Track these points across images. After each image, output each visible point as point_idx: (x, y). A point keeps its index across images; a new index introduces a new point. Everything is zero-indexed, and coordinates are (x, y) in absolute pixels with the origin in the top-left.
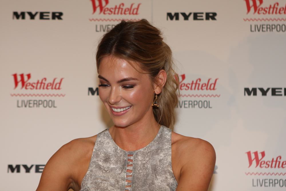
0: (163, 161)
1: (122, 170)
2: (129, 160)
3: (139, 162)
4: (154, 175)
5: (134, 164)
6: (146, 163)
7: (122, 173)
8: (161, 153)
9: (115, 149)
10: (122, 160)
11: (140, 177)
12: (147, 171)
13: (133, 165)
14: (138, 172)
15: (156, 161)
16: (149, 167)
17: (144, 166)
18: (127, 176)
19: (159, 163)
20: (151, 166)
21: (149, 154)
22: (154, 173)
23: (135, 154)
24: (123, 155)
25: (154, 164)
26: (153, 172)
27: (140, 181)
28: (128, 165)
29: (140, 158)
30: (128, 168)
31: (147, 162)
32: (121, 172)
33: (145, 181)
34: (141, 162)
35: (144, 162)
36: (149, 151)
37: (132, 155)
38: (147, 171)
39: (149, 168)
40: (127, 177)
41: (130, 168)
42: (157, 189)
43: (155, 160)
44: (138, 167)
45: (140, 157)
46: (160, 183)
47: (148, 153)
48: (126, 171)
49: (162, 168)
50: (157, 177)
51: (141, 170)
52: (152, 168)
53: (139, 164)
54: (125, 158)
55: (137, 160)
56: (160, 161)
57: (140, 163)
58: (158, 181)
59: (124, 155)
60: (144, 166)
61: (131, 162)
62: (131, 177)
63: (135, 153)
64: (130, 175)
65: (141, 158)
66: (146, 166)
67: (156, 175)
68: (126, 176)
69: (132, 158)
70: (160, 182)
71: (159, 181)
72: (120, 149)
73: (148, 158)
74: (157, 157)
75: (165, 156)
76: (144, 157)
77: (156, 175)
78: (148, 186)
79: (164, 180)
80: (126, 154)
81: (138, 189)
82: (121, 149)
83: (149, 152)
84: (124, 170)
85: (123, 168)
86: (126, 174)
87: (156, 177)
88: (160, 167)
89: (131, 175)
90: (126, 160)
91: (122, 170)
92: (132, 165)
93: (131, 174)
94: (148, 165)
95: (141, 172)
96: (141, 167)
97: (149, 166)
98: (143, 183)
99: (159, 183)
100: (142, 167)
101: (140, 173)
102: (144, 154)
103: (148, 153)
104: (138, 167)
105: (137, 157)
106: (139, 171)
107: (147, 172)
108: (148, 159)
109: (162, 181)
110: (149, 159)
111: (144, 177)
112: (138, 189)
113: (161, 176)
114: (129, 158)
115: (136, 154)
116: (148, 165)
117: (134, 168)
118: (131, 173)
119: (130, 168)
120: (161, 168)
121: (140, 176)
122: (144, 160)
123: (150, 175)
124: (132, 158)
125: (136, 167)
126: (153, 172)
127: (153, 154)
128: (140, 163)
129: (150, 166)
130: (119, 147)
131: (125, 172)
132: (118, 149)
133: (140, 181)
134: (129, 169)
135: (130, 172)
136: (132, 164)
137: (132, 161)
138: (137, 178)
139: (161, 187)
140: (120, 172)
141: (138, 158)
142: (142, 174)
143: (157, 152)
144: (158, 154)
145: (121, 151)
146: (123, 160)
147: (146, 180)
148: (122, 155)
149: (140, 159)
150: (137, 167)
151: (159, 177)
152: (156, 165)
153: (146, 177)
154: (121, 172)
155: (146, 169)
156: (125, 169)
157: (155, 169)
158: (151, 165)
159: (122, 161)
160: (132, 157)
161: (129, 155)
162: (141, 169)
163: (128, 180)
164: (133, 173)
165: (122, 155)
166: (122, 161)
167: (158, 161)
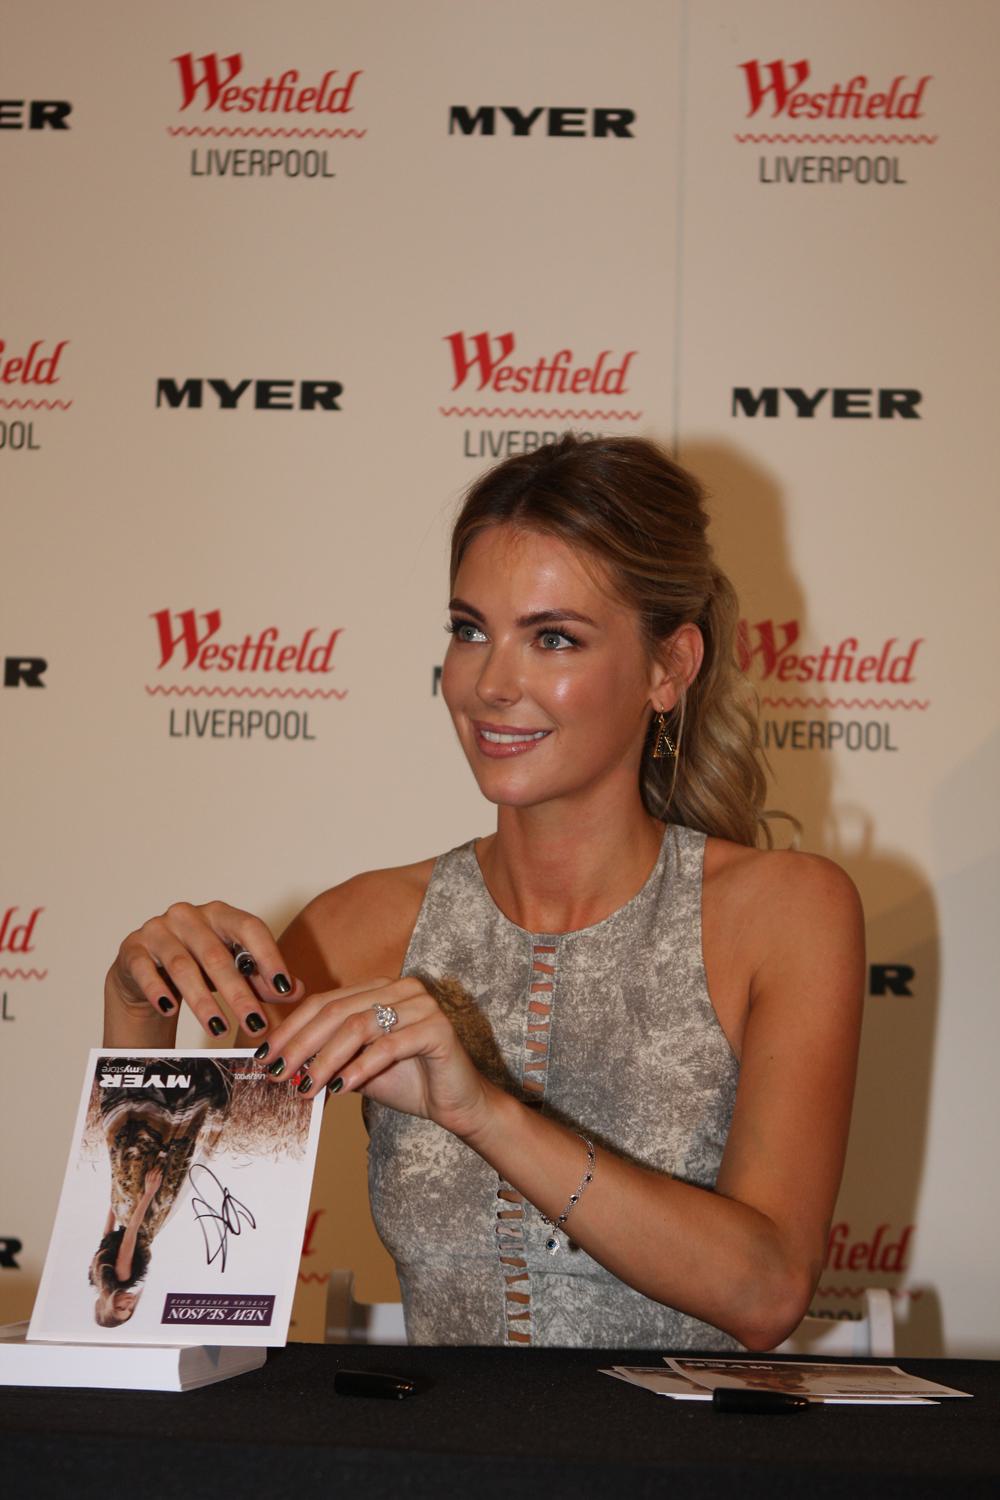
0: (673, 970)
1: (512, 1005)
2: (538, 965)
4: (637, 1029)
5: (558, 983)
6: (607, 977)
7: (511, 1016)
8: (662, 939)
9: (491, 922)
10: (510, 962)
12: (607, 1009)
13: (555, 986)
14: (570, 1011)
15: (644, 972)
16: (613, 995)
17: (595, 990)
18: (529, 1026)
19: (654, 980)
20: (624, 995)
21: (618, 947)
22: (637, 1020)
24: (515, 946)
25: (638, 985)
26: (632, 1018)
27: (578, 1047)
28: (535, 988)
29: (581, 960)
30: (533, 997)
31: (612, 974)
32: (509, 1011)
33: (597, 1049)
34: (586, 976)
35: (597, 975)
36: (619, 935)
37: (552, 950)
38: (607, 1009)
39: (615, 998)
41: (544, 997)
44: (574, 993)
46: (659, 1059)
49: (671, 998)
50: (650, 1033)
51: (584, 1004)
52: (627, 1002)
53: (578, 982)
54: (525, 959)
55: (569, 968)
56: (660, 970)
57: (580, 977)
58: (651, 1049)
59: (519, 947)
61: (545, 976)
63: (564, 942)
64: (543, 1023)
65: (586, 962)
66: (604, 990)
68: (525, 1028)
70: (656, 1055)
71: (656, 1048)
72: (504, 924)
74: (648, 955)
75: (677, 952)
76: (600, 960)
77: (643, 1027)
78: (609, 1069)
80: (526, 943)
82: (508, 923)
83: (617, 940)
84: (520, 1004)
86: (526, 1018)
87: (645, 1036)
88: (663, 992)
90: (525, 967)
91: (512, 1005)
92: (548, 986)
93: (547, 1020)
94: (614, 988)
96: (583, 994)
97: (616, 991)
98: (590, 1053)
99: (654, 1058)
102: (599, 948)
104: (572, 995)
106: (574, 1008)
107: (605, 1014)
108: (614, 963)
109: (664, 1051)
110: (619, 964)
111: (593, 1031)
113: (667, 1030)
114: (541, 957)
115: (567, 947)
116: (614, 988)
117: (559, 999)
118: (547, 1017)
119: (544, 997)
120: (664, 999)
121: (580, 1025)
122: (598, 969)
123: (620, 1030)
124: (551, 959)
126: (632, 1018)
127: (633, 944)
128: (580, 977)
129: (621, 990)
130: (502, 916)
131: (523, 1012)
132: (500, 923)
133: (578, 1047)
135: (543, 1015)
137: (549, 970)
139: (658, 1074)
140: (504, 1011)
141: (575, 962)
142: (587, 1019)
145: (508, 932)
146: (517, 964)
147: (602, 1046)
148: (510, 944)
151: (657, 1034)
152: (644, 990)
153: (603, 1035)
154: (509, 1011)
155: (604, 999)
156: (524, 1003)
157: (637, 1002)
160: (550, 955)
161: (537, 949)
163: (534, 1042)
164: (553, 1018)
165: (510, 944)
167: (651, 972)
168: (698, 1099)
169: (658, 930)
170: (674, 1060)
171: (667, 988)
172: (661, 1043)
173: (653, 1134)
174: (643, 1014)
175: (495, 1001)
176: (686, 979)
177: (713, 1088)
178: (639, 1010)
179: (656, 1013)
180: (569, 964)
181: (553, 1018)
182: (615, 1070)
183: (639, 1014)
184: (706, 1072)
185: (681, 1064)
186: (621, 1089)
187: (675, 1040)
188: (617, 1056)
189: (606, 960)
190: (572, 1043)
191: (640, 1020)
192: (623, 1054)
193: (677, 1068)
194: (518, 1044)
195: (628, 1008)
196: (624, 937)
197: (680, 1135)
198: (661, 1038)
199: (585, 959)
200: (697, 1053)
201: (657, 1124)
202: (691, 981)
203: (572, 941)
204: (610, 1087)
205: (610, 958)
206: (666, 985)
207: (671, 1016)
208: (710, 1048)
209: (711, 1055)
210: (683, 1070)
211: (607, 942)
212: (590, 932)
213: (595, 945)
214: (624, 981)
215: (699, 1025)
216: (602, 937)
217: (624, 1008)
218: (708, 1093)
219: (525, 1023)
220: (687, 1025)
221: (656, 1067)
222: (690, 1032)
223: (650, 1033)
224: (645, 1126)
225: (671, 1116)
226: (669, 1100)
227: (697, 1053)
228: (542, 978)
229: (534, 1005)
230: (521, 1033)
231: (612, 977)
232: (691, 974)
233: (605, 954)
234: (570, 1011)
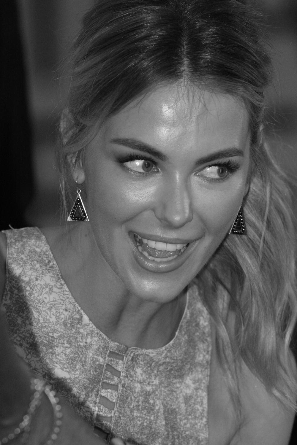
2: (109, 367)
6: (154, 392)
11: (132, 430)
16: (157, 408)
17: (146, 401)
19: (183, 406)
20: (164, 412)
23: (130, 358)
24: (95, 347)
30: (103, 393)
34: (142, 388)
35: (149, 388)
36: (168, 360)
38: (152, 418)
43: (175, 394)
44: (133, 398)
45: (139, 371)
47: (160, 365)
51: (138, 410)
52: (166, 419)
53: (137, 390)
55: (131, 376)
56: (187, 399)
59: (99, 348)
60: (146, 401)
64: (109, 416)
65: (142, 375)
66: (151, 402)
69: (120, 366)
73: (157, 378)
83: (164, 363)
84: (94, 397)
88: (188, 419)
89: (111, 417)
90: (101, 366)
92: (115, 387)
94: (158, 402)
95: (137, 417)
96: (138, 402)
97: (159, 406)
100: (140, 403)
101: (133, 419)
103: (160, 365)
104: (131, 400)
105: (134, 367)
106: (132, 411)
117: (123, 400)
121: (134, 426)
122: (149, 384)
125: (127, 398)
128: (138, 386)
129: (162, 407)
134: (109, 397)
137: (117, 373)
141: (135, 373)
142: (139, 423)
146: (94, 362)
149: (140, 378)
150: (129, 399)
155: (151, 409)
156: (97, 395)
158: (165, 407)
159: (88, 365)
160: (121, 362)
161: (112, 354)
162: (139, 406)
164: (117, 414)
166: (88, 365)
167: (181, 399)
171: (190, 417)
179: (184, 435)
180: (132, 373)
181: (117, 414)
183: (173, 432)
195: (167, 424)
203: (137, 355)
206: (190, 415)
214: (164, 399)
217: (164, 423)
228: (113, 379)
231: (157, 393)
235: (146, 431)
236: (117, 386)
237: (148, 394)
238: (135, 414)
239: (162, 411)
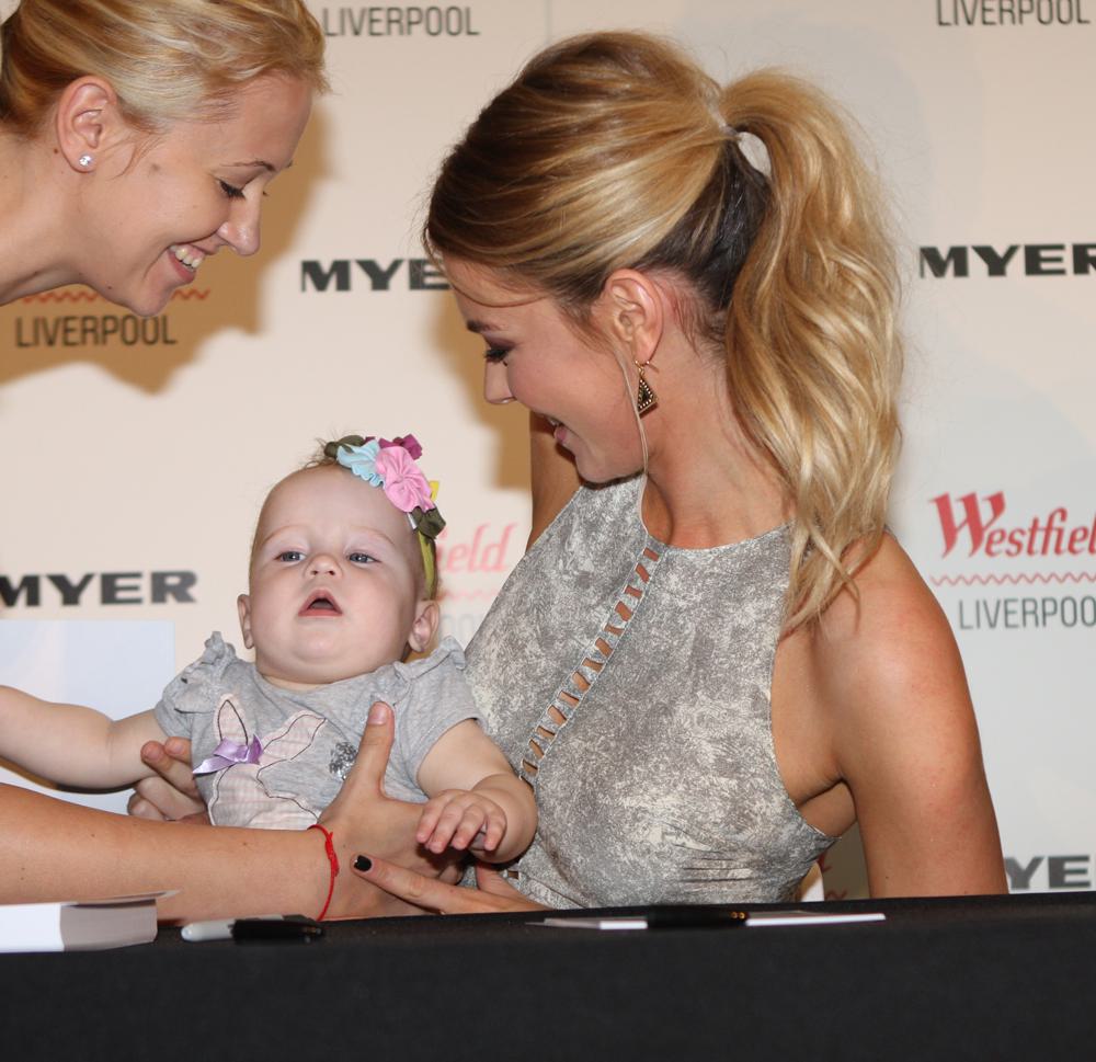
1: (603, 598)
3: (664, 595)
4: (689, 683)
5: (647, 594)
6: (688, 610)
7: (597, 609)
10: (621, 556)
13: (643, 596)
14: (644, 628)
16: (687, 632)
17: (673, 619)
19: (727, 639)
20: (696, 639)
21: (709, 581)
24: (632, 540)
26: (690, 669)
27: (635, 667)
28: (630, 590)
32: (598, 604)
33: (650, 678)
35: (681, 604)
36: (716, 570)
38: (675, 643)
40: (606, 629)
41: (632, 603)
42: (668, 738)
43: (720, 620)
45: (674, 578)
46: (692, 724)
47: (706, 577)
48: (614, 606)
50: (699, 693)
52: (694, 649)
53: (663, 602)
54: (633, 556)
56: (737, 632)
60: (673, 619)
62: (615, 636)
64: (619, 627)
65: (677, 584)
67: (696, 684)
68: (603, 625)
69: (651, 567)
70: (692, 719)
71: (695, 713)
74: (731, 611)
75: (759, 622)
77: (696, 684)
78: (649, 706)
79: (712, 720)
81: (615, 691)
83: (712, 574)
85: (612, 590)
86: (608, 615)
87: (693, 694)
88: (728, 657)
90: (630, 565)
91: (603, 598)
92: (637, 593)
94: (689, 625)
106: (649, 628)
108: (699, 598)
110: (704, 601)
112: (615, 691)
117: (642, 611)
118: (625, 623)
119: (632, 603)
122: (684, 598)
125: (648, 610)
127: (723, 588)
128: (666, 598)
129: (694, 633)
133: (635, 667)
136: (641, 592)
137: (645, 576)
138: (633, 653)
140: (594, 602)
141: (668, 579)
142: (654, 644)
143: (740, 588)
144: (739, 600)
151: (704, 698)
153: (661, 667)
154: (598, 604)
155: (677, 631)
156: (614, 600)
157: (702, 651)
158: (698, 632)
160: (652, 562)
167: (727, 630)
168: (712, 784)
169: (753, 589)
170: (705, 733)
171: (733, 656)
172: (702, 710)
173: (646, 790)
174: (702, 671)
175: (592, 588)
176: (754, 656)
177: (731, 778)
178: (700, 664)
180: (663, 579)
182: (653, 711)
184: (729, 760)
185: (710, 742)
186: (647, 733)
187: (715, 714)
188: (662, 700)
189: (694, 592)
190: (632, 660)
191: (696, 675)
192: (666, 701)
193: (704, 743)
194: (591, 637)
195: (692, 656)
196: (719, 575)
197: (673, 806)
198: (705, 705)
199: (677, 580)
200: (729, 738)
201: (656, 784)
202: (758, 661)
204: (640, 723)
205: (698, 591)
207: (724, 688)
208: (744, 738)
209: (741, 746)
210: (708, 748)
211: (701, 572)
212: (690, 555)
213: (690, 569)
215: (744, 712)
216: (699, 564)
217: (689, 653)
218: (723, 780)
219: (606, 620)
220: (733, 706)
221: (686, 730)
222: (733, 713)
223: (699, 693)
224: (644, 779)
225: (675, 786)
226: (681, 769)
227: (729, 738)
229: (622, 608)
230: (597, 628)
232: (761, 654)
233: (695, 584)
234: (644, 628)
235: (661, 657)
236: (641, 592)
237: (678, 611)
238: (653, 632)
239: (692, 637)
